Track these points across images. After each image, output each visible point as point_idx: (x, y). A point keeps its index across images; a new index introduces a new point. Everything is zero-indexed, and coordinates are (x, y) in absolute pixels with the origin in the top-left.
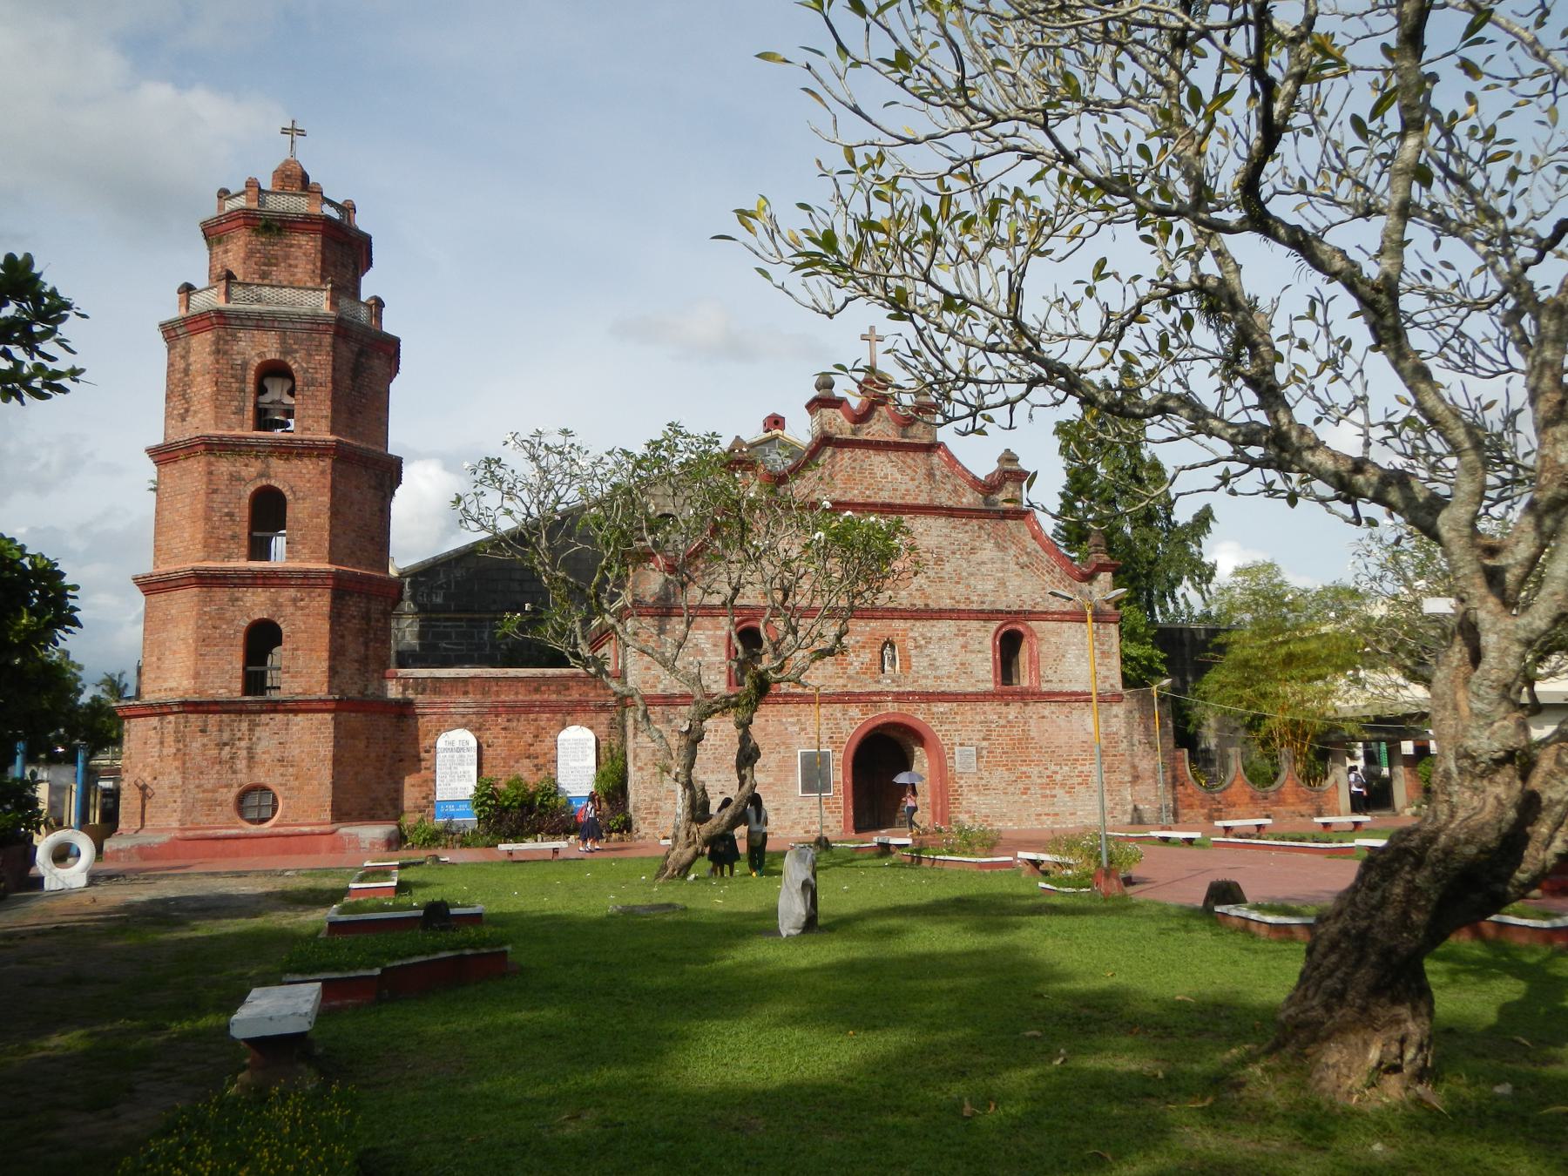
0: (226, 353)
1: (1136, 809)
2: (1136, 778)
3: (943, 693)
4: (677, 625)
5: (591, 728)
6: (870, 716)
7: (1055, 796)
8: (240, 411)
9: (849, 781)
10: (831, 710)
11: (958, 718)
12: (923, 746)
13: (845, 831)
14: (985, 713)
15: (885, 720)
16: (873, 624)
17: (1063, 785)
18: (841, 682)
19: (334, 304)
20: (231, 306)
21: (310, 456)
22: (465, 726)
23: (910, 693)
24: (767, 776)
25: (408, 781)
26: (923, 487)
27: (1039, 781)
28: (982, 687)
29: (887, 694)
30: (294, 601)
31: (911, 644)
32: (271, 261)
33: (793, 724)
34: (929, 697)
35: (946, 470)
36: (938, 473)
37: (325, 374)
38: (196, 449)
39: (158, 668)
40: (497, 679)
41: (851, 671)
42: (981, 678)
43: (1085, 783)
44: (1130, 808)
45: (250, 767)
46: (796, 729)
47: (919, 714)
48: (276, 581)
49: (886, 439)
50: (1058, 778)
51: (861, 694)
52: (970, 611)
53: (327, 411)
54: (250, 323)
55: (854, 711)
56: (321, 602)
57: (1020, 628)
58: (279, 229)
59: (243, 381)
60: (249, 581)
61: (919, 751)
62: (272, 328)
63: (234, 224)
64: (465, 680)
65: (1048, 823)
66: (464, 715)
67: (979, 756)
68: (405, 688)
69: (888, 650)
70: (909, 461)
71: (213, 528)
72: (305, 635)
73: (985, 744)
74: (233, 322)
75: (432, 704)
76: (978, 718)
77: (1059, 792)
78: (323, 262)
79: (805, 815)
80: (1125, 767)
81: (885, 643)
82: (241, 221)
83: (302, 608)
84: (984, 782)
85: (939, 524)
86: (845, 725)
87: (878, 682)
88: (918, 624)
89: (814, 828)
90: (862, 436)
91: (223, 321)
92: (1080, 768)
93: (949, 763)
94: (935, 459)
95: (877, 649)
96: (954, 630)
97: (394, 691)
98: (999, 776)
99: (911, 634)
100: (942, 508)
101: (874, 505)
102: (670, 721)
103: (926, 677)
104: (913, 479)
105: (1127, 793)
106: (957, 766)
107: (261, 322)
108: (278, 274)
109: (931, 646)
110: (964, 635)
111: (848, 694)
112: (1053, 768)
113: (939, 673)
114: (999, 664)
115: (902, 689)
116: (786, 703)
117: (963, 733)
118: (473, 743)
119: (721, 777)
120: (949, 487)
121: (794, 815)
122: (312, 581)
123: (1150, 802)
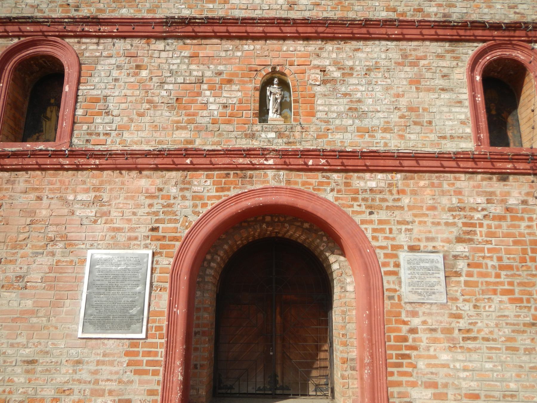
3: (374, 155)
6: (233, 193)
9: (180, 311)
10: (158, 182)
11: (406, 201)
12: (343, 254)
14: (459, 192)
15: (260, 200)
16: (249, 46)
23: (306, 154)
24: (23, 297)
28: (450, 147)
29: (264, 153)
33: (85, 204)
41: (203, 119)
42: (448, 133)
46: (91, 212)
52: (422, 24)
57: (520, 55)
69: (274, 89)
73: (461, 248)
76: (445, 201)
79: (85, 376)
81: (268, 82)
84: (463, 324)
87: (253, 136)
88: (329, 46)
93: (388, 282)
95: (258, 81)
96: (395, 55)
99: (316, 62)
103: (345, 130)
106: (405, 290)
109: (353, 81)
110: (413, 64)
111: (187, 153)
113: (367, 123)
114: (482, 112)
116: (78, 168)
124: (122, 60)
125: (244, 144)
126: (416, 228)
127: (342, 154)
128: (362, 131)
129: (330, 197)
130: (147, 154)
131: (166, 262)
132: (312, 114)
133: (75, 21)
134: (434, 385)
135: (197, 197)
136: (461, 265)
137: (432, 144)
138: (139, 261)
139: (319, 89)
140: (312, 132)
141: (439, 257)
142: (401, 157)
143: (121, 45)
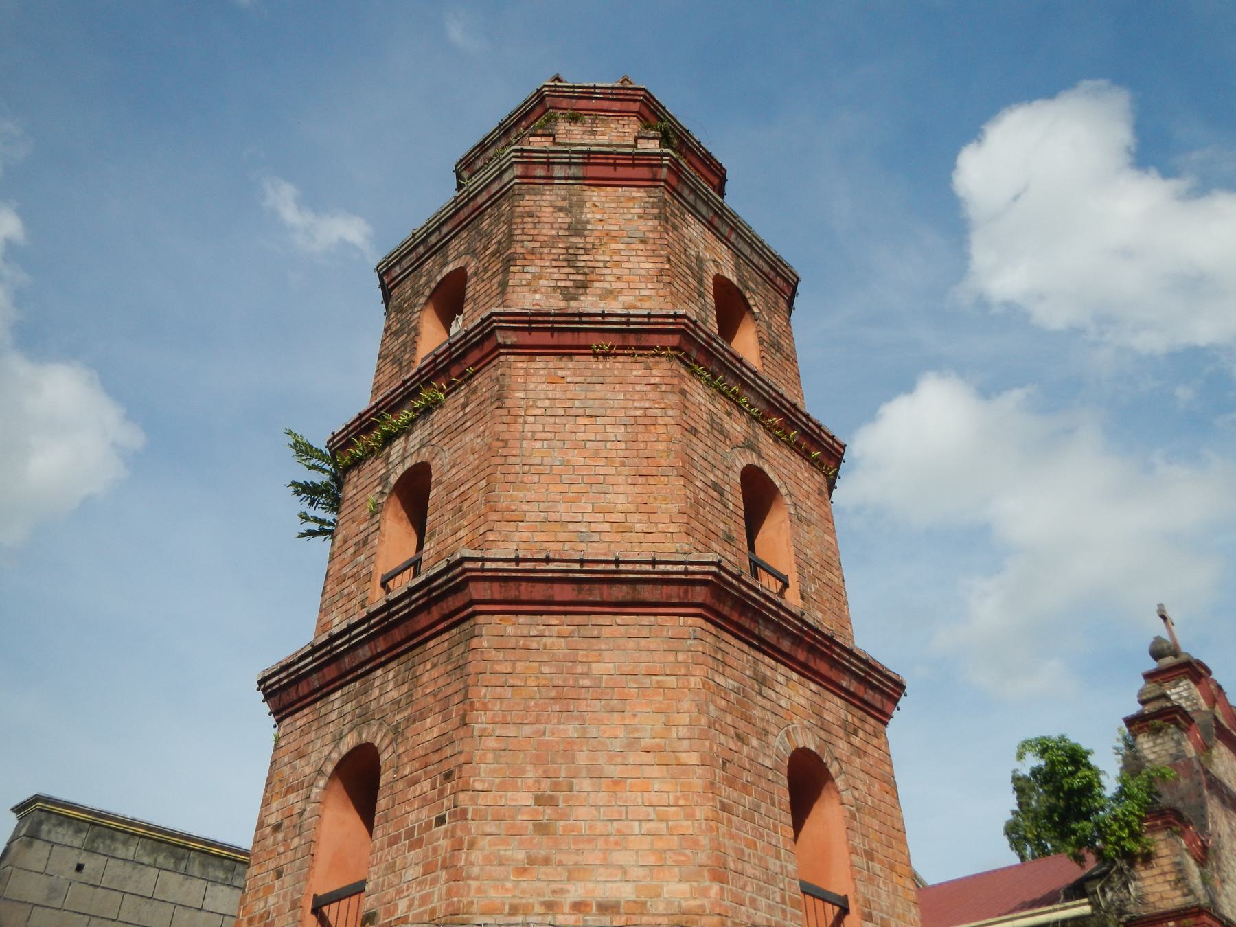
0: (675, 228)
21: (805, 455)
30: (844, 725)
38: (655, 340)
39: (542, 828)
48: (823, 667)
54: (703, 210)
60: (786, 645)
63: (617, 106)
71: (697, 501)
72: (875, 823)
74: (686, 192)
82: (636, 106)
83: (860, 753)
91: (674, 182)
122: (869, 695)
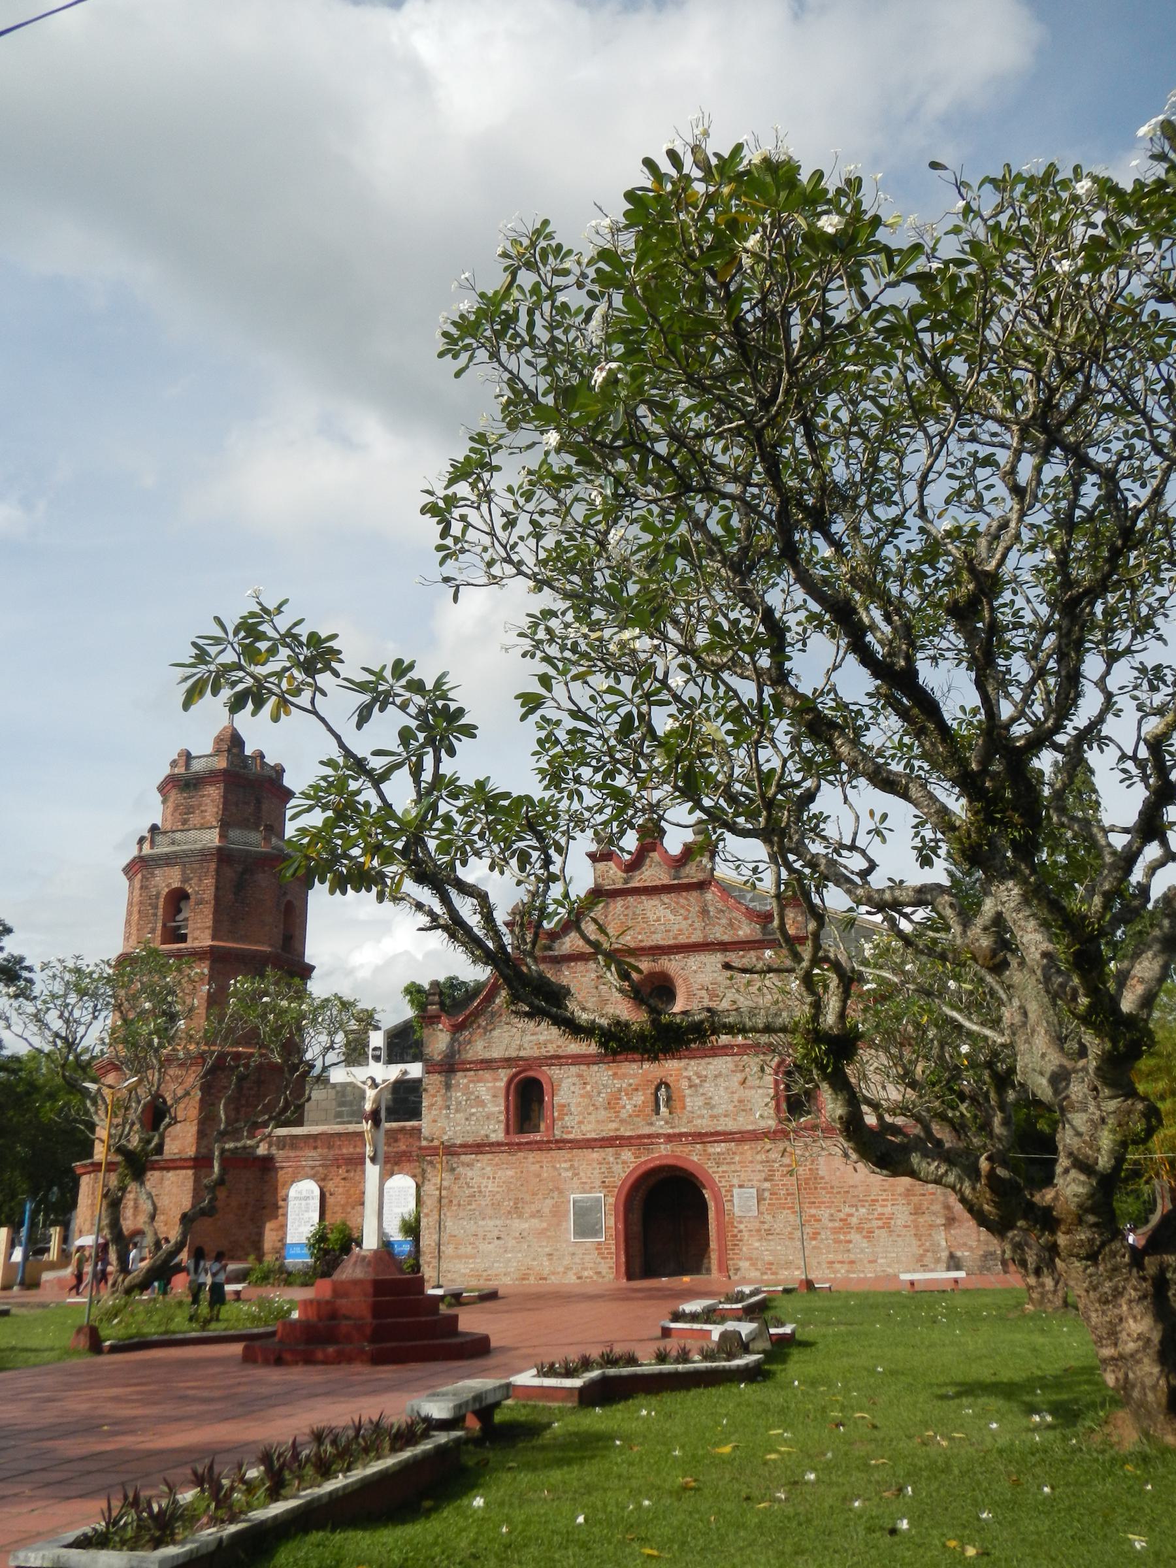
1: (952, 1256)
2: (951, 1221)
3: (717, 1134)
4: (460, 1079)
5: (414, 1176)
7: (850, 1242)
8: (153, 931)
9: (621, 1226)
11: (737, 1158)
13: (617, 1278)
17: (859, 1229)
18: (614, 1125)
19: (222, 836)
20: (156, 851)
22: (312, 1177)
23: (681, 1135)
25: (269, 1226)
26: (697, 925)
27: (830, 1225)
29: (658, 1136)
31: (685, 1084)
32: (190, 810)
33: (566, 1170)
34: (701, 1137)
35: (720, 905)
36: (711, 909)
37: (209, 895)
40: (339, 1135)
41: (624, 1114)
43: (886, 1226)
44: (944, 1255)
45: (135, 1215)
46: (569, 1174)
47: (694, 1157)
49: (658, 883)
50: (854, 1221)
51: (630, 1137)
53: (210, 923)
55: (627, 1155)
56: (193, 1077)
58: (195, 785)
59: (156, 908)
61: (707, 1194)
62: (176, 864)
64: (315, 1137)
65: (842, 1271)
66: (313, 1168)
67: (760, 1199)
68: (270, 1146)
70: (682, 901)
73: (767, 1185)
75: (288, 1159)
76: (758, 1157)
77: (855, 1237)
78: (225, 804)
80: (937, 1207)
85: (714, 960)
86: (618, 1169)
87: (651, 1124)
88: (692, 1063)
89: (586, 1274)
90: (634, 884)
92: (880, 1210)
93: (727, 1206)
94: (709, 896)
96: (731, 1066)
97: (262, 1150)
98: (785, 1220)
100: (713, 944)
101: (643, 949)
102: (453, 1170)
103: (702, 1117)
104: (686, 919)
105: (941, 1237)
106: (736, 1210)
107: (168, 860)
108: (194, 820)
111: (617, 1138)
112: (847, 1210)
113: (715, 1112)
115: (677, 1131)
117: (743, 1174)
118: (317, 1192)
119: (498, 1222)
120: (724, 921)
121: (567, 1261)
123: (971, 1249)
124: (575, 1080)
125: (647, 1130)
126: (743, 1174)
127: (700, 1135)
128: (713, 1117)
129: (695, 1159)
130: (595, 1140)
131: (612, 1200)
132: (684, 1108)
133: (547, 1058)
134: (750, 1259)
135: (624, 1162)
136: (767, 1194)
137: (752, 1123)
138: (598, 1200)
139: (687, 1092)
140: (685, 1120)
141: (754, 1191)
142: (732, 1133)
143: (574, 1069)
